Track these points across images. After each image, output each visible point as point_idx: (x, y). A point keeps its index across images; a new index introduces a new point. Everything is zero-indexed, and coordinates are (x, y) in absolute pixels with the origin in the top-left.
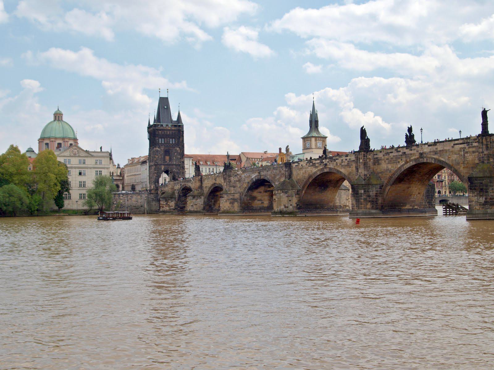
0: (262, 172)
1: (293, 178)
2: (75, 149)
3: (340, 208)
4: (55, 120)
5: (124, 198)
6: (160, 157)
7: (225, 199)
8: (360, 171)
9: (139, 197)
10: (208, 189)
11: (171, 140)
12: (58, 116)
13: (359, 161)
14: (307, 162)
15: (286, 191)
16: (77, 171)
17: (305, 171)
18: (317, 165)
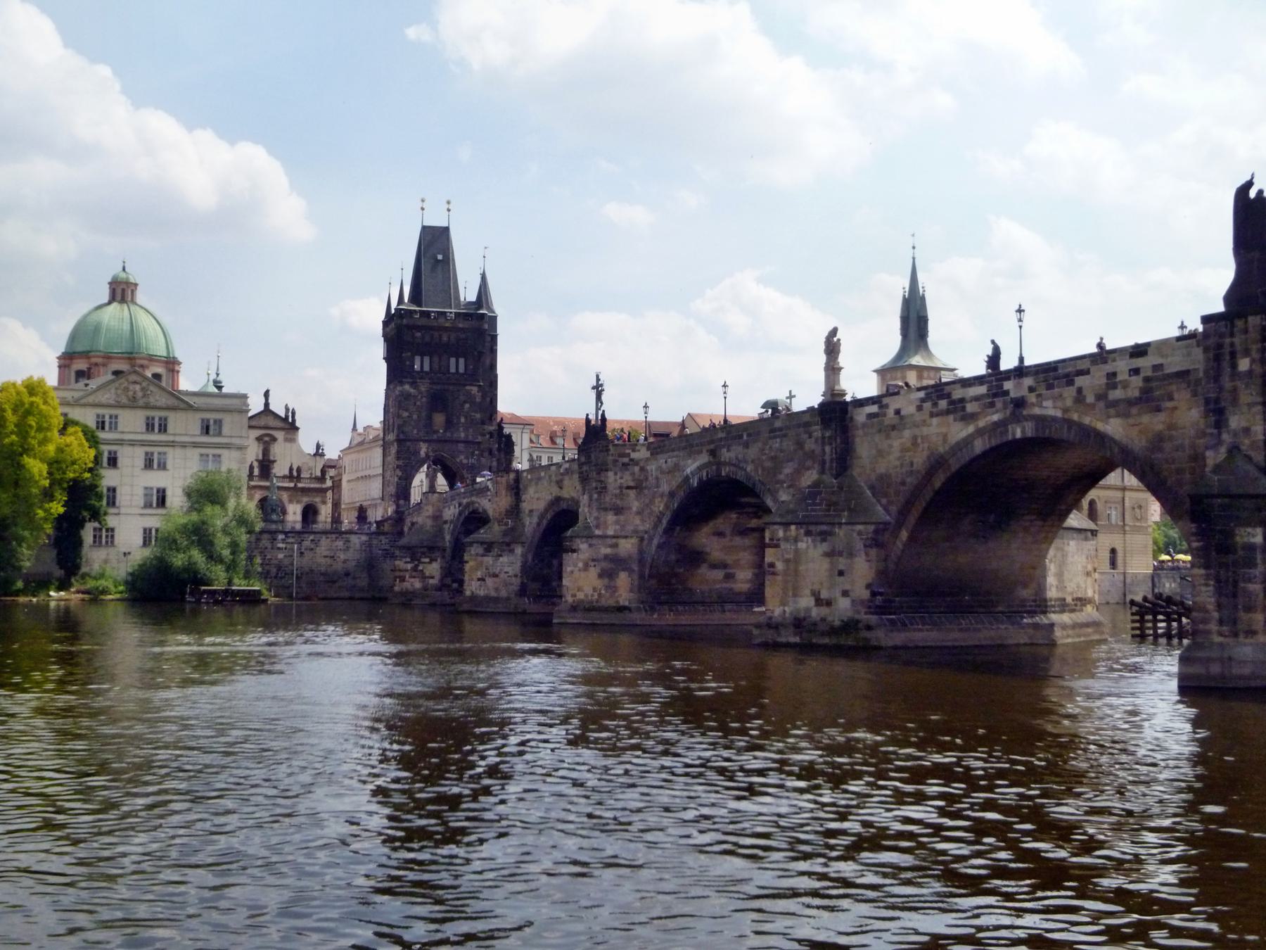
0: (725, 450)
1: (856, 472)
2: (135, 382)
3: (1062, 612)
4: (113, 299)
5: (288, 546)
6: (415, 417)
7: (582, 556)
8: (1235, 422)
9: (340, 544)
10: (535, 520)
11: (453, 360)
12: (121, 291)
13: (1227, 370)
14: (922, 394)
15: (824, 528)
16: (140, 453)
17: (915, 438)
18: (971, 408)
